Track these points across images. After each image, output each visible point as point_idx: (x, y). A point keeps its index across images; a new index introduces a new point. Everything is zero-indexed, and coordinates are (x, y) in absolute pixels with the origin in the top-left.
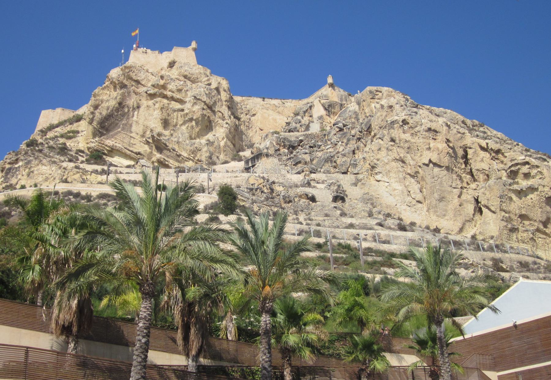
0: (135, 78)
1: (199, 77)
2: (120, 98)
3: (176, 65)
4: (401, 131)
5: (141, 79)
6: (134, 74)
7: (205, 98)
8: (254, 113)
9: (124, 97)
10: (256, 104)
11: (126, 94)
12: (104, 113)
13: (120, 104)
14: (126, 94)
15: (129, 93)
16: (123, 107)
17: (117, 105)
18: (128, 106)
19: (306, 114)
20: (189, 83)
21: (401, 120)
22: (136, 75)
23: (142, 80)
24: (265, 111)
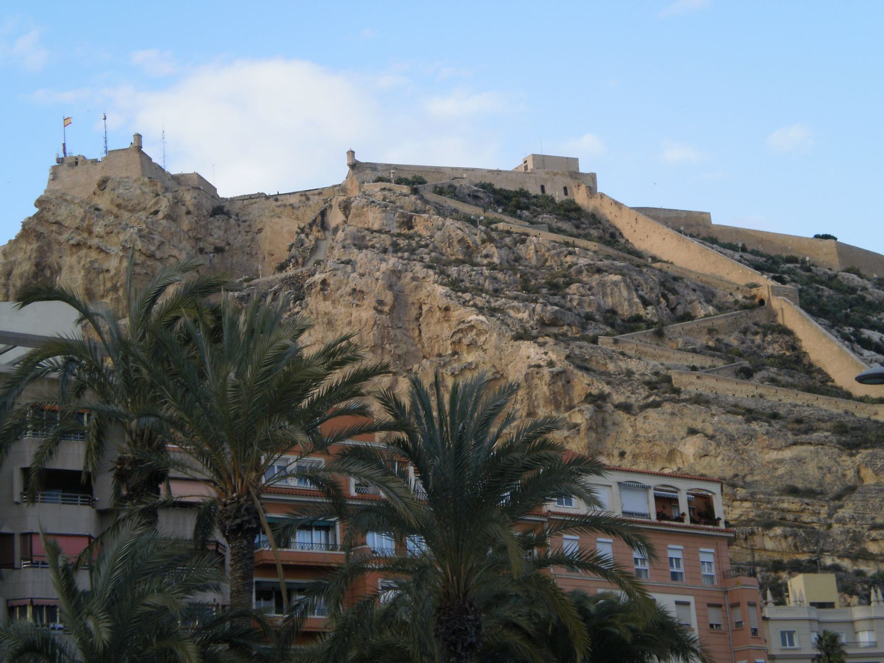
0: (52, 219)
1: (142, 200)
2: (36, 257)
3: (110, 185)
4: (320, 297)
5: (63, 218)
6: (51, 213)
7: (139, 245)
8: (260, 226)
9: (42, 253)
10: (264, 209)
11: (46, 248)
12: (19, 283)
13: (37, 265)
14: (46, 248)
15: (49, 244)
16: (43, 270)
17: (34, 268)
18: (49, 267)
19: (314, 228)
20: (126, 215)
21: (320, 281)
22: (54, 214)
23: (64, 220)
24: (276, 220)
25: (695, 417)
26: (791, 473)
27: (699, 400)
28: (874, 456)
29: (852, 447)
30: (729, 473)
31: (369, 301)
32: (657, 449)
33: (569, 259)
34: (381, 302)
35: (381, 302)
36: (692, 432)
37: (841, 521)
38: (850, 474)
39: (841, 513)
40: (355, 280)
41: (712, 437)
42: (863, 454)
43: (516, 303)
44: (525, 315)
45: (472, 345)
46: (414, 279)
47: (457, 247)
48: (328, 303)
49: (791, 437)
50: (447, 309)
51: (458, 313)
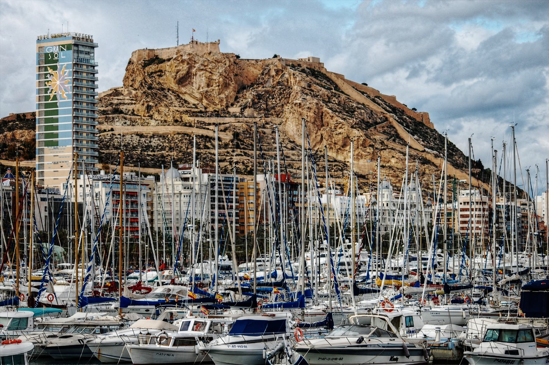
0: (194, 60)
7: (224, 74)
25: (393, 153)
26: (412, 168)
27: (392, 149)
28: (429, 167)
29: (423, 164)
30: (401, 167)
31: (312, 111)
32: (386, 160)
33: (350, 103)
34: (315, 111)
35: (315, 111)
36: (393, 157)
37: (425, 181)
38: (423, 170)
39: (424, 179)
40: (308, 105)
41: (397, 159)
42: (426, 166)
43: (349, 118)
44: (352, 121)
45: (341, 128)
46: (321, 106)
47: (326, 97)
48: (301, 109)
49: (413, 161)
50: (333, 116)
51: (336, 118)
